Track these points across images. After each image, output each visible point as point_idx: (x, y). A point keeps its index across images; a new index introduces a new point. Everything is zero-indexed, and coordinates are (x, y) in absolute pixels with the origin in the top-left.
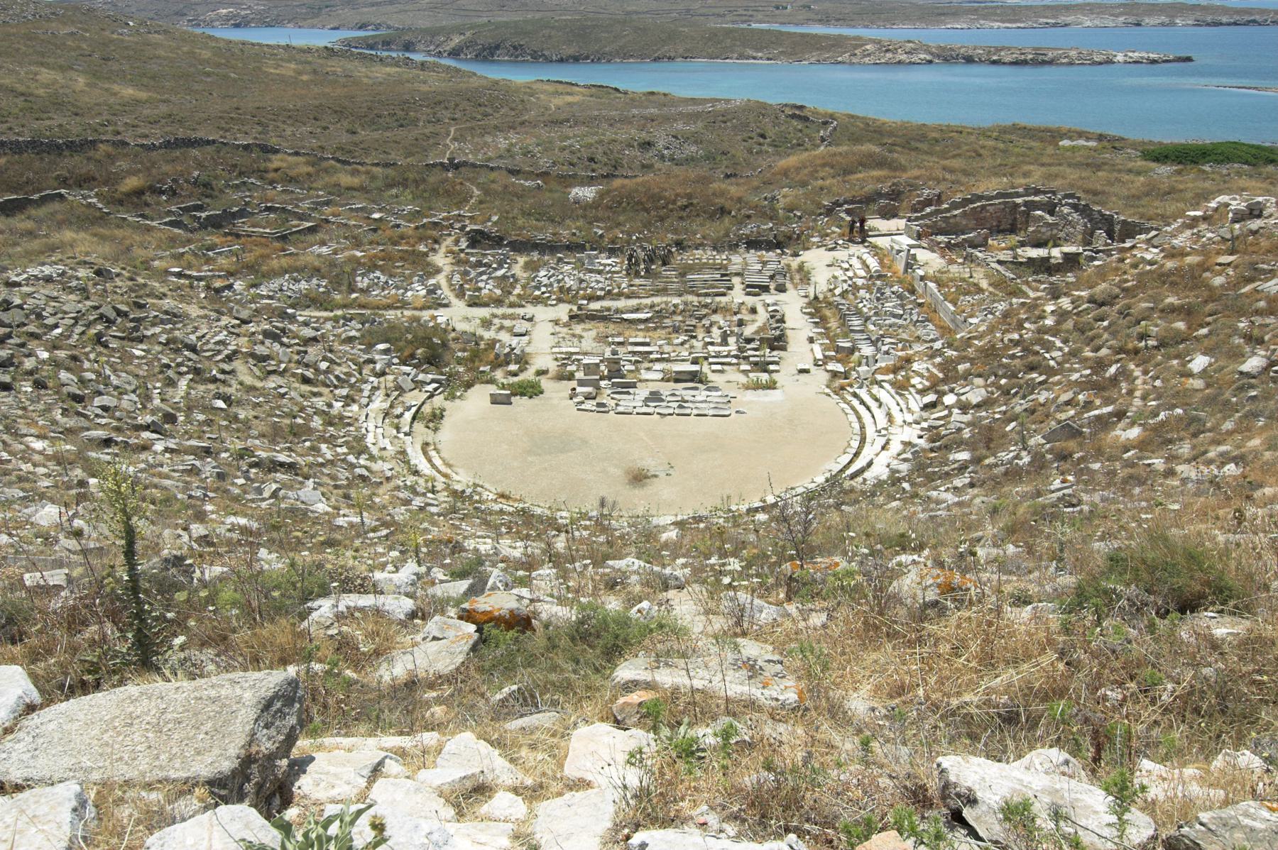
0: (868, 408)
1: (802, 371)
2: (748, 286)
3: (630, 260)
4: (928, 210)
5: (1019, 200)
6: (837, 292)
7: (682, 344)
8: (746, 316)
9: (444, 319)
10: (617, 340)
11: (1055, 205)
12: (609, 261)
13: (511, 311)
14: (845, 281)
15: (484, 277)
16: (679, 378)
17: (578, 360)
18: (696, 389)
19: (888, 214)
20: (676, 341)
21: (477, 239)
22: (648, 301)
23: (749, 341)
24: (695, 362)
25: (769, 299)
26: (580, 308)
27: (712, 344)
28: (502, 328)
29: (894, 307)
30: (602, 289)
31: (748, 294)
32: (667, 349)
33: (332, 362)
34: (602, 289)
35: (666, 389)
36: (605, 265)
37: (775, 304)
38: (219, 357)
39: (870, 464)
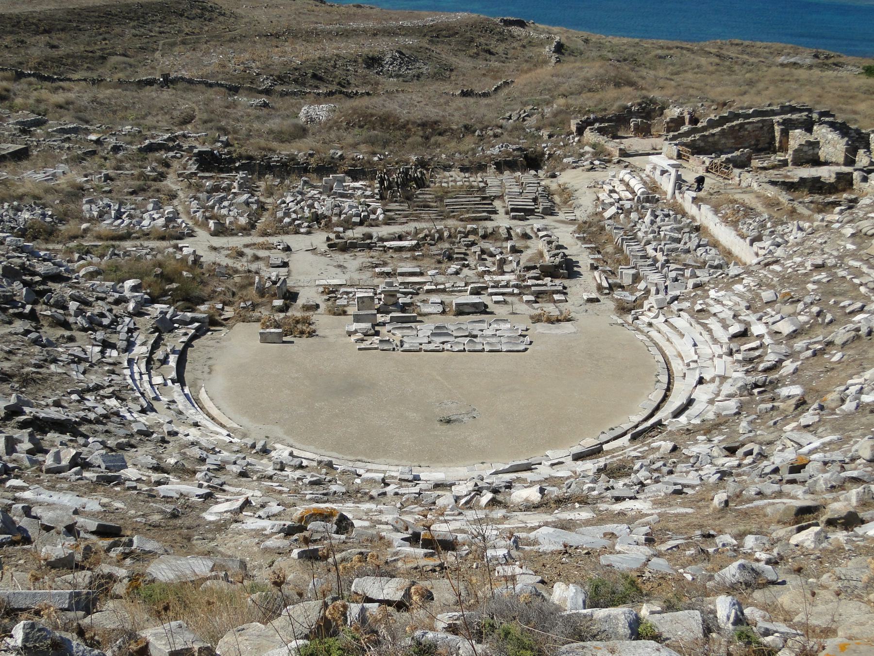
1: (591, 300)
2: (513, 210)
4: (685, 128)
5: (777, 118)
6: (607, 214)
7: (457, 273)
8: (519, 244)
9: (191, 250)
14: (612, 204)
15: (226, 203)
16: (461, 310)
17: (347, 293)
19: (644, 131)
20: (450, 271)
21: (208, 162)
22: (411, 227)
23: (528, 269)
24: (476, 292)
25: (536, 223)
26: (338, 237)
27: (489, 272)
28: (257, 258)
29: (672, 230)
30: (358, 215)
31: (514, 218)
32: (440, 279)
34: (358, 215)
35: (451, 323)
36: (354, 189)
37: (545, 229)
39: (690, 402)
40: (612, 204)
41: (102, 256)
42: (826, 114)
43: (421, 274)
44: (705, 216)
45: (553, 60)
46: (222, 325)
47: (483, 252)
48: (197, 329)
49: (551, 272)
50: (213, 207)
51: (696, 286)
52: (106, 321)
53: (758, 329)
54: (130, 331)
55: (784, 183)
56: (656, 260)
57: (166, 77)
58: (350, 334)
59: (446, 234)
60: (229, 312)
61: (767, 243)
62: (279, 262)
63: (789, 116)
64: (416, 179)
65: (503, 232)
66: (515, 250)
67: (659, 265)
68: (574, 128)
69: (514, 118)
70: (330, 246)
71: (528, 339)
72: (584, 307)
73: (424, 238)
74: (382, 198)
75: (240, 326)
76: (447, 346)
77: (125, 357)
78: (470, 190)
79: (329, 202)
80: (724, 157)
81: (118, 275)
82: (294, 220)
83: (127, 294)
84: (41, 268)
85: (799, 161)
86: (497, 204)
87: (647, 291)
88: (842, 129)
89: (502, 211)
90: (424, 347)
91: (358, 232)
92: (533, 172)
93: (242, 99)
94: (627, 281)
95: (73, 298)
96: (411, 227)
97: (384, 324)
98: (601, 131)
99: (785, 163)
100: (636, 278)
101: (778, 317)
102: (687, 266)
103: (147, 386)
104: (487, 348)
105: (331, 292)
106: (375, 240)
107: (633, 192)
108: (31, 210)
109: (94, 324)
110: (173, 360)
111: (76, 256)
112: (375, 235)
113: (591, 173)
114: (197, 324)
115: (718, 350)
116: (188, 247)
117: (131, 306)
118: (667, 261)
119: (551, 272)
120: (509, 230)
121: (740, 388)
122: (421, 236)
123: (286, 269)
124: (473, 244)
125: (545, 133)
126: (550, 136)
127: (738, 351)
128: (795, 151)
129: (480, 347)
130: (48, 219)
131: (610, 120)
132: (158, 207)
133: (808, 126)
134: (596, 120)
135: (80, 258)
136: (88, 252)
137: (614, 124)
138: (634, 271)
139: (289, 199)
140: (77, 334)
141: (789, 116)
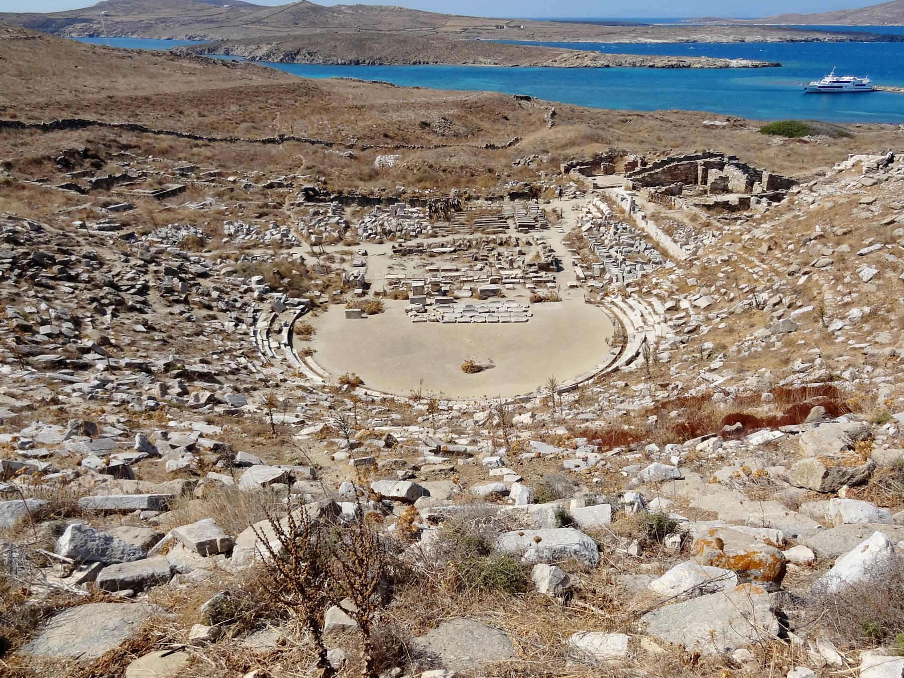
0: (624, 312)
1: (572, 287)
2: (520, 226)
3: (430, 208)
4: (637, 169)
5: (700, 161)
6: (584, 228)
7: (481, 269)
8: (524, 250)
10: (432, 268)
11: (724, 164)
12: (414, 210)
13: (347, 248)
14: (588, 221)
15: (322, 224)
18: (498, 302)
19: (609, 171)
21: (311, 196)
23: (530, 265)
24: (494, 282)
25: (535, 234)
26: (400, 245)
27: (502, 268)
28: (343, 260)
29: (628, 239)
30: (414, 231)
31: (521, 231)
32: (470, 273)
33: (222, 291)
34: (414, 231)
35: (477, 303)
36: (412, 212)
37: (542, 239)
38: (133, 291)
40: (588, 221)
41: (237, 260)
42: (734, 158)
43: (457, 270)
44: (651, 228)
45: (550, 124)
46: (319, 307)
47: (499, 254)
48: (303, 310)
49: (545, 267)
50: (314, 225)
51: (643, 276)
52: (238, 305)
53: (684, 304)
54: (256, 311)
55: (704, 205)
56: (617, 260)
57: (282, 137)
58: (407, 311)
59: (474, 242)
60: (325, 298)
61: (691, 246)
62: (359, 263)
63: (708, 160)
64: (453, 206)
65: (513, 241)
66: (521, 253)
67: (619, 262)
68: (562, 169)
69: (522, 163)
70: (395, 252)
71: (529, 314)
72: (568, 292)
73: (460, 246)
74: (431, 217)
75: (332, 307)
76: (473, 319)
77: (252, 328)
78: (492, 213)
79: (394, 221)
80: (664, 188)
81: (247, 272)
82: (370, 234)
83: (254, 286)
84: (194, 269)
85: (715, 190)
86: (510, 222)
87: (611, 280)
88: (744, 168)
89: (512, 226)
90: (458, 320)
91: (413, 243)
92: (535, 200)
93: (333, 151)
94: (597, 273)
95: (216, 289)
96: (450, 238)
97: (431, 304)
98: (582, 172)
99: (705, 192)
100: (603, 271)
101: (698, 296)
102: (637, 262)
103: (267, 348)
104: (501, 320)
105: (395, 283)
106: (425, 247)
107: (602, 213)
108: (187, 229)
109: (230, 307)
110: (285, 330)
111: (219, 261)
112: (425, 244)
113: (574, 201)
114: (302, 306)
115: (657, 319)
116: (297, 253)
117: (256, 294)
118: (624, 260)
119: (545, 267)
120: (517, 240)
121: (671, 345)
122: (457, 244)
123: (364, 268)
124: (493, 249)
125: (543, 173)
126: (546, 175)
127: (671, 320)
128: (712, 184)
129: (496, 320)
130: (199, 236)
131: (587, 164)
132: (276, 226)
133: (721, 166)
134: (578, 164)
135: (221, 263)
136: (228, 257)
137: (590, 167)
138: (602, 266)
139: (367, 219)
140: (220, 315)
141: (708, 160)
